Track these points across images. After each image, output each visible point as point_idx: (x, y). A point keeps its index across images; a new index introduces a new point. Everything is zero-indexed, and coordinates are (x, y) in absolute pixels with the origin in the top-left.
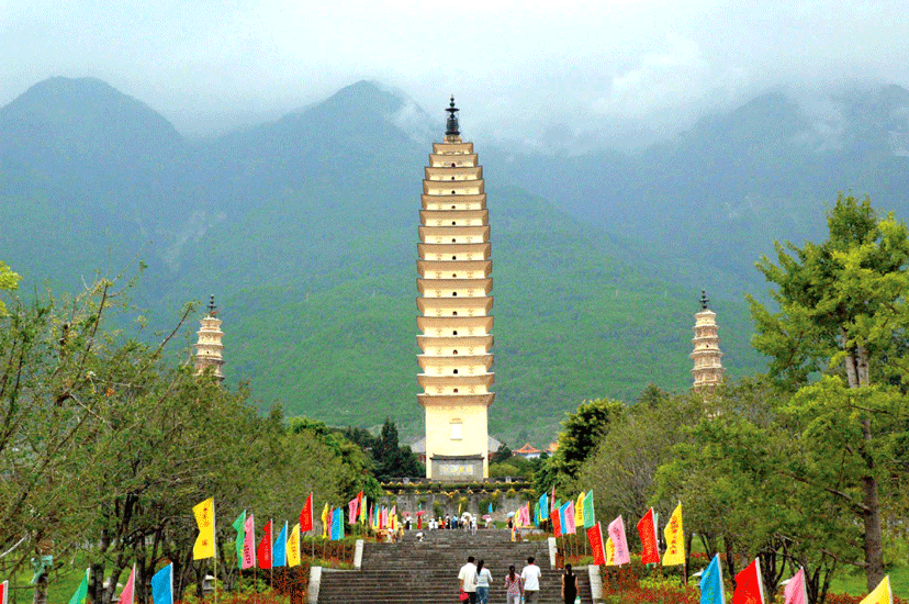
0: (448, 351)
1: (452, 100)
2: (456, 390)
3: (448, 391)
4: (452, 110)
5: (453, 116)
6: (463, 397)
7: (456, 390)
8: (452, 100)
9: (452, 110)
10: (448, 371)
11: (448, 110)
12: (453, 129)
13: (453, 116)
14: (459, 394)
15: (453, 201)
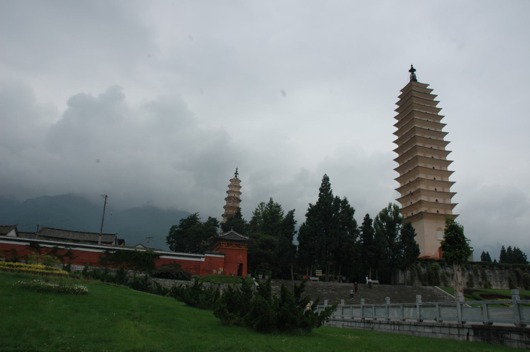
0: (432, 188)
1: (412, 66)
2: (438, 212)
3: (434, 211)
4: (412, 70)
5: (413, 74)
6: (442, 215)
7: (438, 212)
8: (412, 66)
9: (412, 70)
10: (433, 200)
11: (410, 71)
12: (413, 79)
13: (413, 74)
14: (440, 212)
15: (427, 110)
